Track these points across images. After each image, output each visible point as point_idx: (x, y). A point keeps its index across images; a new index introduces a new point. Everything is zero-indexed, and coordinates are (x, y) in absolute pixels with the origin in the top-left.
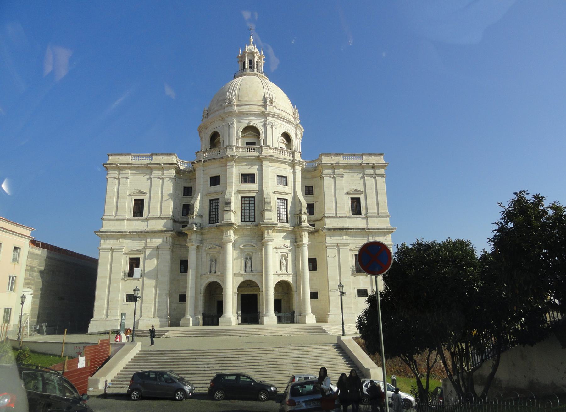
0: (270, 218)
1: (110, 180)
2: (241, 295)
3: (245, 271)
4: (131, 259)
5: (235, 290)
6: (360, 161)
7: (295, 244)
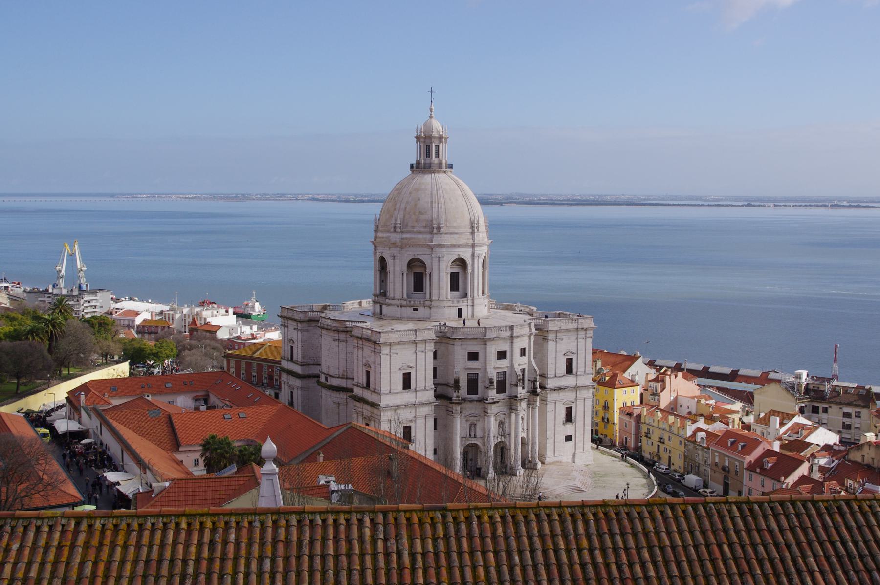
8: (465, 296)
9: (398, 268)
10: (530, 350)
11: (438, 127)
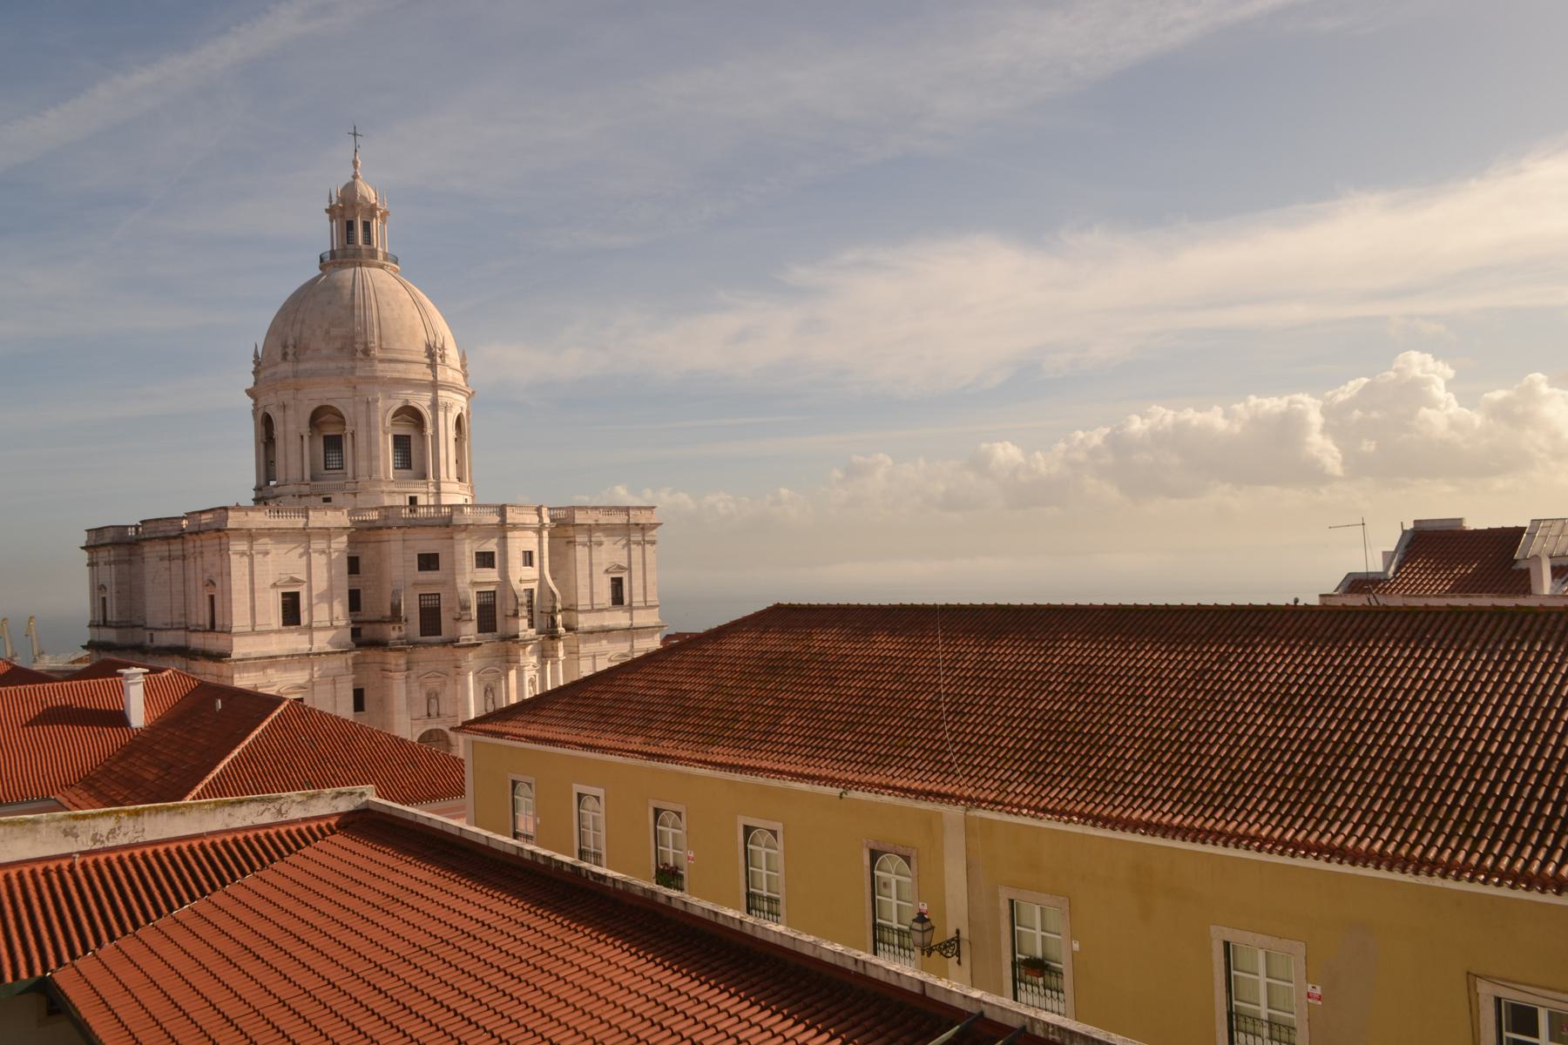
1: (234, 558)
8: (424, 476)
9: (291, 427)
10: (541, 558)
11: (367, 191)
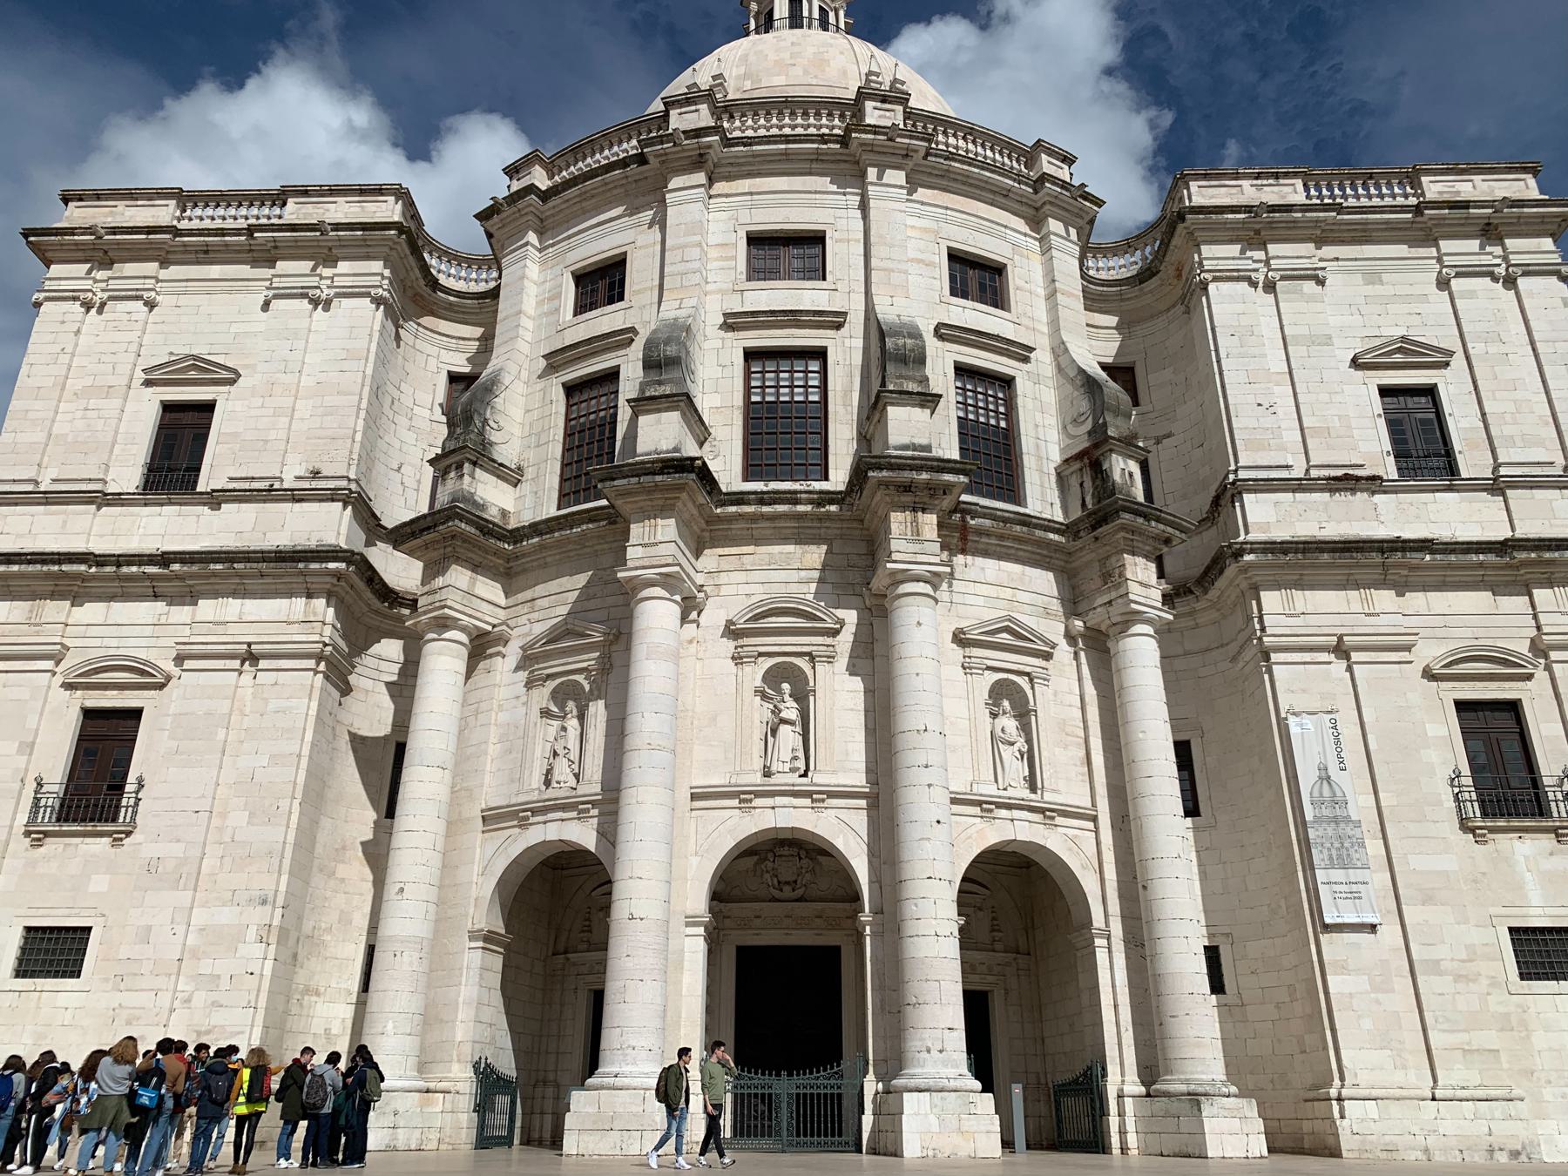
0: (924, 442)
2: (743, 953)
3: (767, 773)
4: (88, 714)
5: (697, 900)
6: (1413, 201)
7: (1079, 623)
